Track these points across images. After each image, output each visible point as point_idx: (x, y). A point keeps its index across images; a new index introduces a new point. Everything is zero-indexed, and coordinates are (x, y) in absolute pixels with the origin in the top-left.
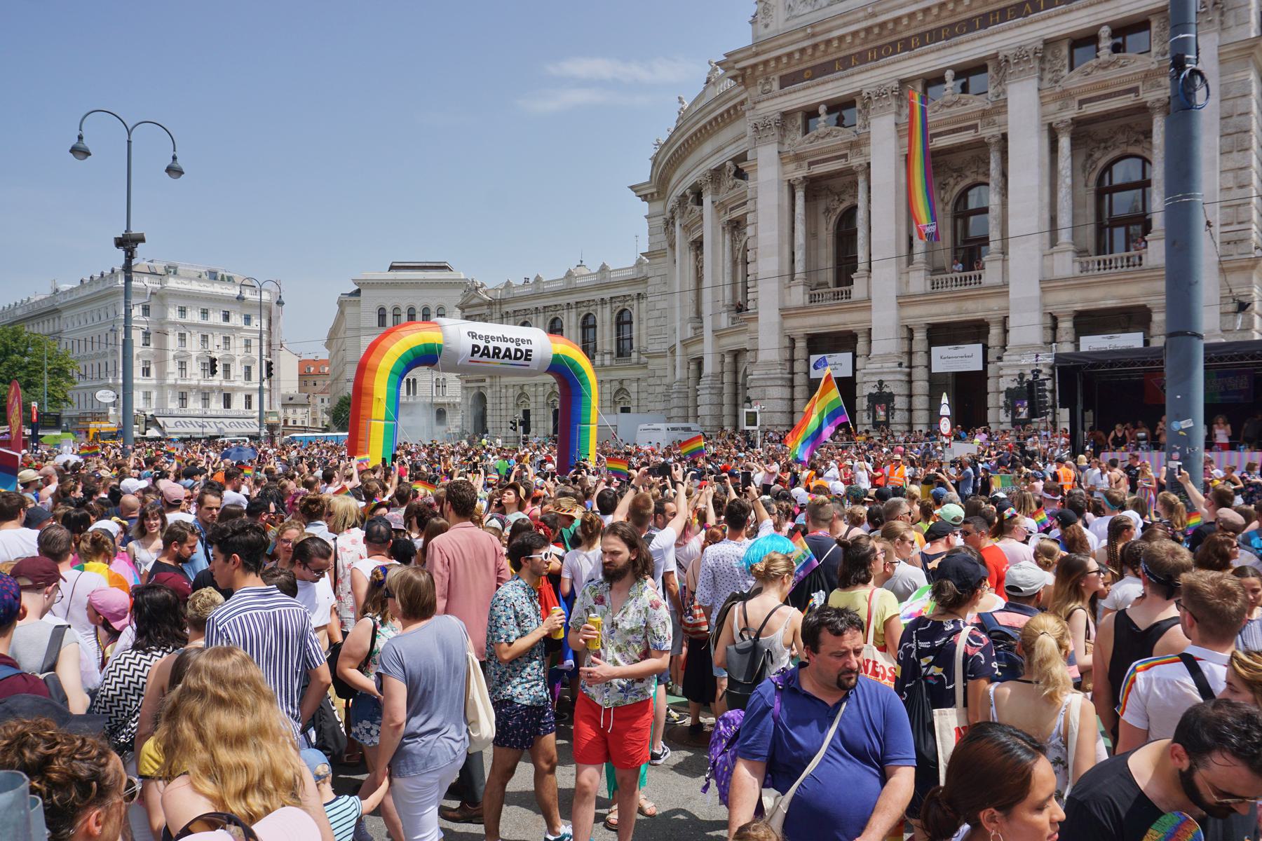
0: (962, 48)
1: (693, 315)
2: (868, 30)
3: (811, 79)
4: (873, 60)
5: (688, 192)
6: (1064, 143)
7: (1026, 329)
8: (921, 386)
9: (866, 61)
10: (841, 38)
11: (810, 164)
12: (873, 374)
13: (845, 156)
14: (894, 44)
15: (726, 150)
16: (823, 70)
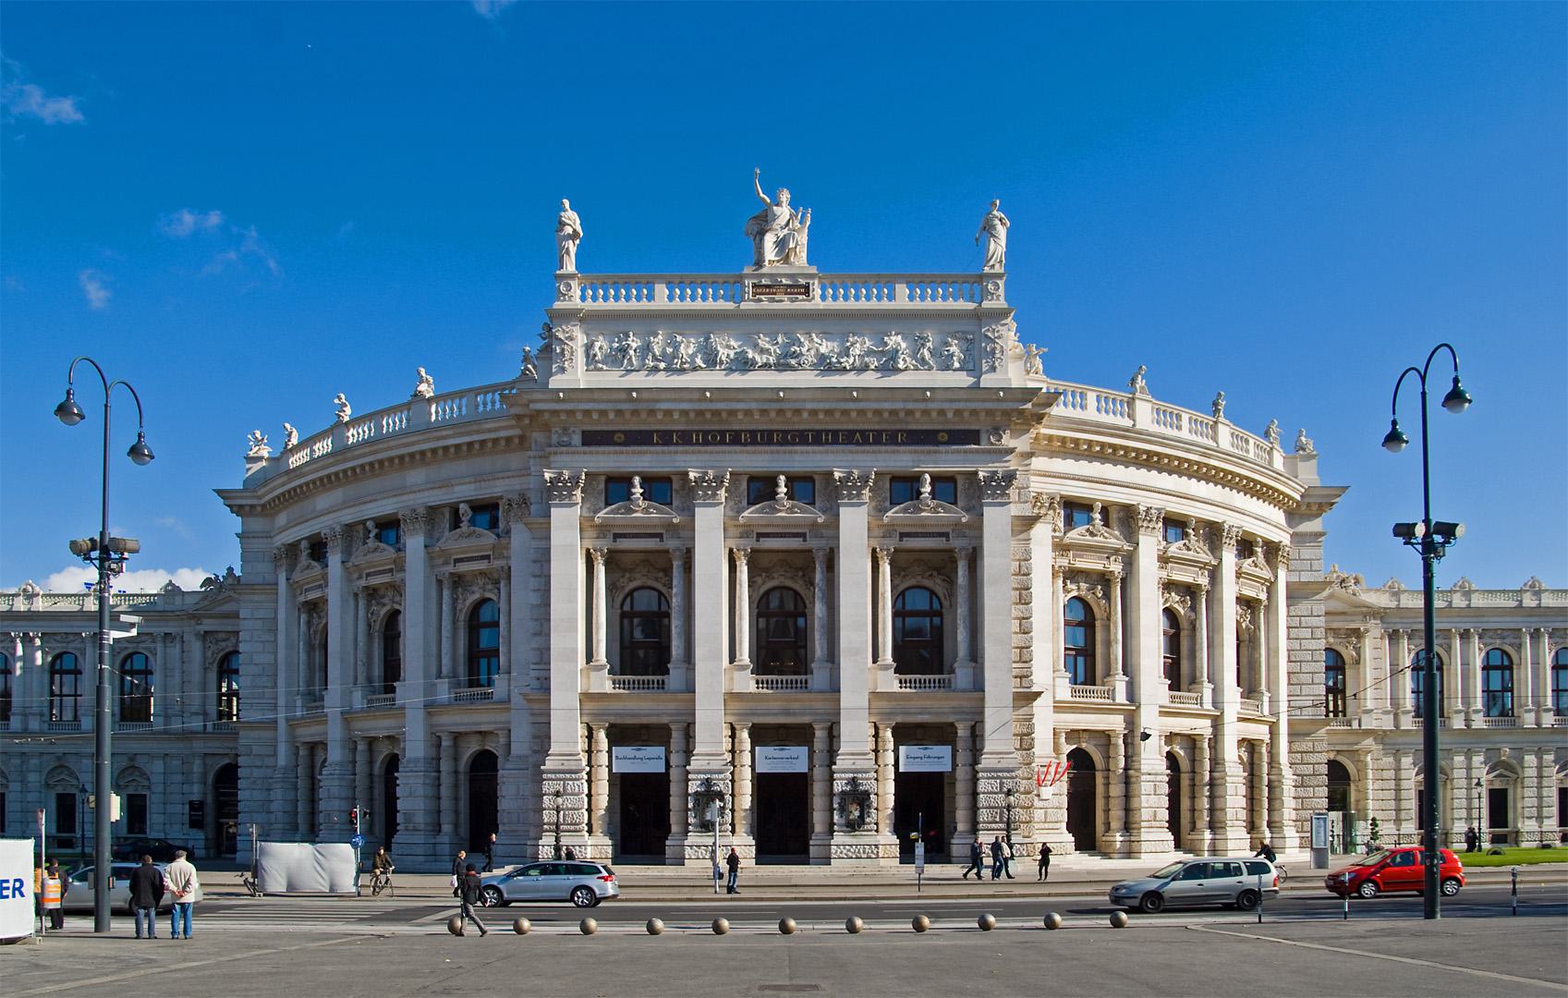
0: (797, 457)
1: (361, 679)
2: (700, 413)
3: (625, 444)
4: (697, 443)
5: (370, 524)
6: (886, 569)
7: (856, 734)
8: (746, 787)
9: (691, 444)
10: (668, 413)
11: (616, 536)
12: (699, 772)
13: (660, 536)
14: (722, 433)
15: (457, 489)
16: (639, 438)
